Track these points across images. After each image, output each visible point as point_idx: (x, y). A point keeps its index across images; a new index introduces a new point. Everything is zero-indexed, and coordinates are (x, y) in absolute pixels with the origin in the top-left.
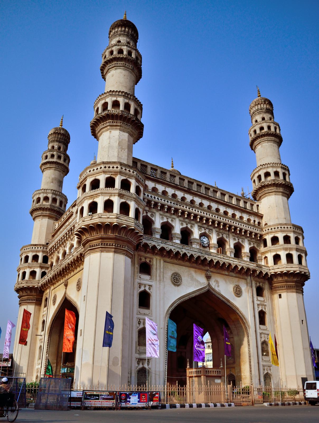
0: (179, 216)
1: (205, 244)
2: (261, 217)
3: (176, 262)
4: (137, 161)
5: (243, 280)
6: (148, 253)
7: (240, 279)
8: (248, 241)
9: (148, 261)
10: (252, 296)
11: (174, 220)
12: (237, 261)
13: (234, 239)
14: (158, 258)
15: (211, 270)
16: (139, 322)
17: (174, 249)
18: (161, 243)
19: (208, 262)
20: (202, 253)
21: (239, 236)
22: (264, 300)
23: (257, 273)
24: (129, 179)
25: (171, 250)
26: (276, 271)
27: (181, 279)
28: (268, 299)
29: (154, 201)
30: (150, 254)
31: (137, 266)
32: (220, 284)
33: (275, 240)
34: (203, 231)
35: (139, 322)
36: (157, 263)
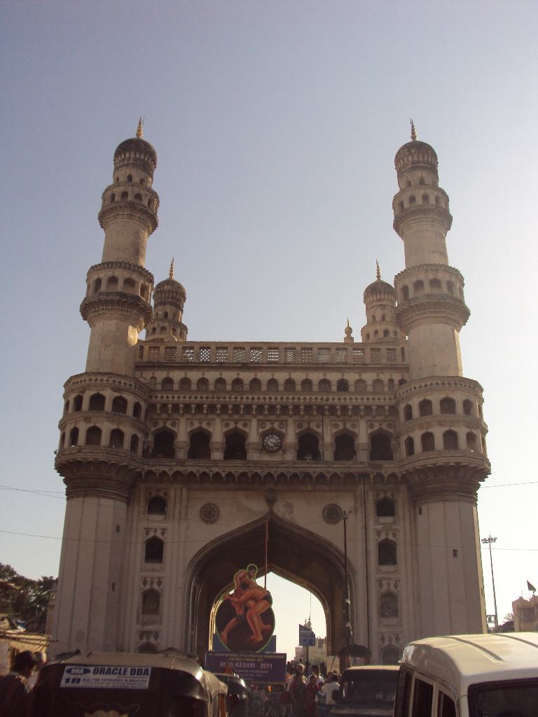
0: (219, 415)
2: (406, 369)
4: (158, 345)
8: (367, 421)
9: (161, 494)
10: (365, 518)
11: (212, 422)
13: (336, 426)
21: (347, 418)
22: (394, 522)
24: (101, 392)
27: (219, 512)
28: (404, 520)
31: (142, 503)
34: (268, 426)
36: (175, 494)
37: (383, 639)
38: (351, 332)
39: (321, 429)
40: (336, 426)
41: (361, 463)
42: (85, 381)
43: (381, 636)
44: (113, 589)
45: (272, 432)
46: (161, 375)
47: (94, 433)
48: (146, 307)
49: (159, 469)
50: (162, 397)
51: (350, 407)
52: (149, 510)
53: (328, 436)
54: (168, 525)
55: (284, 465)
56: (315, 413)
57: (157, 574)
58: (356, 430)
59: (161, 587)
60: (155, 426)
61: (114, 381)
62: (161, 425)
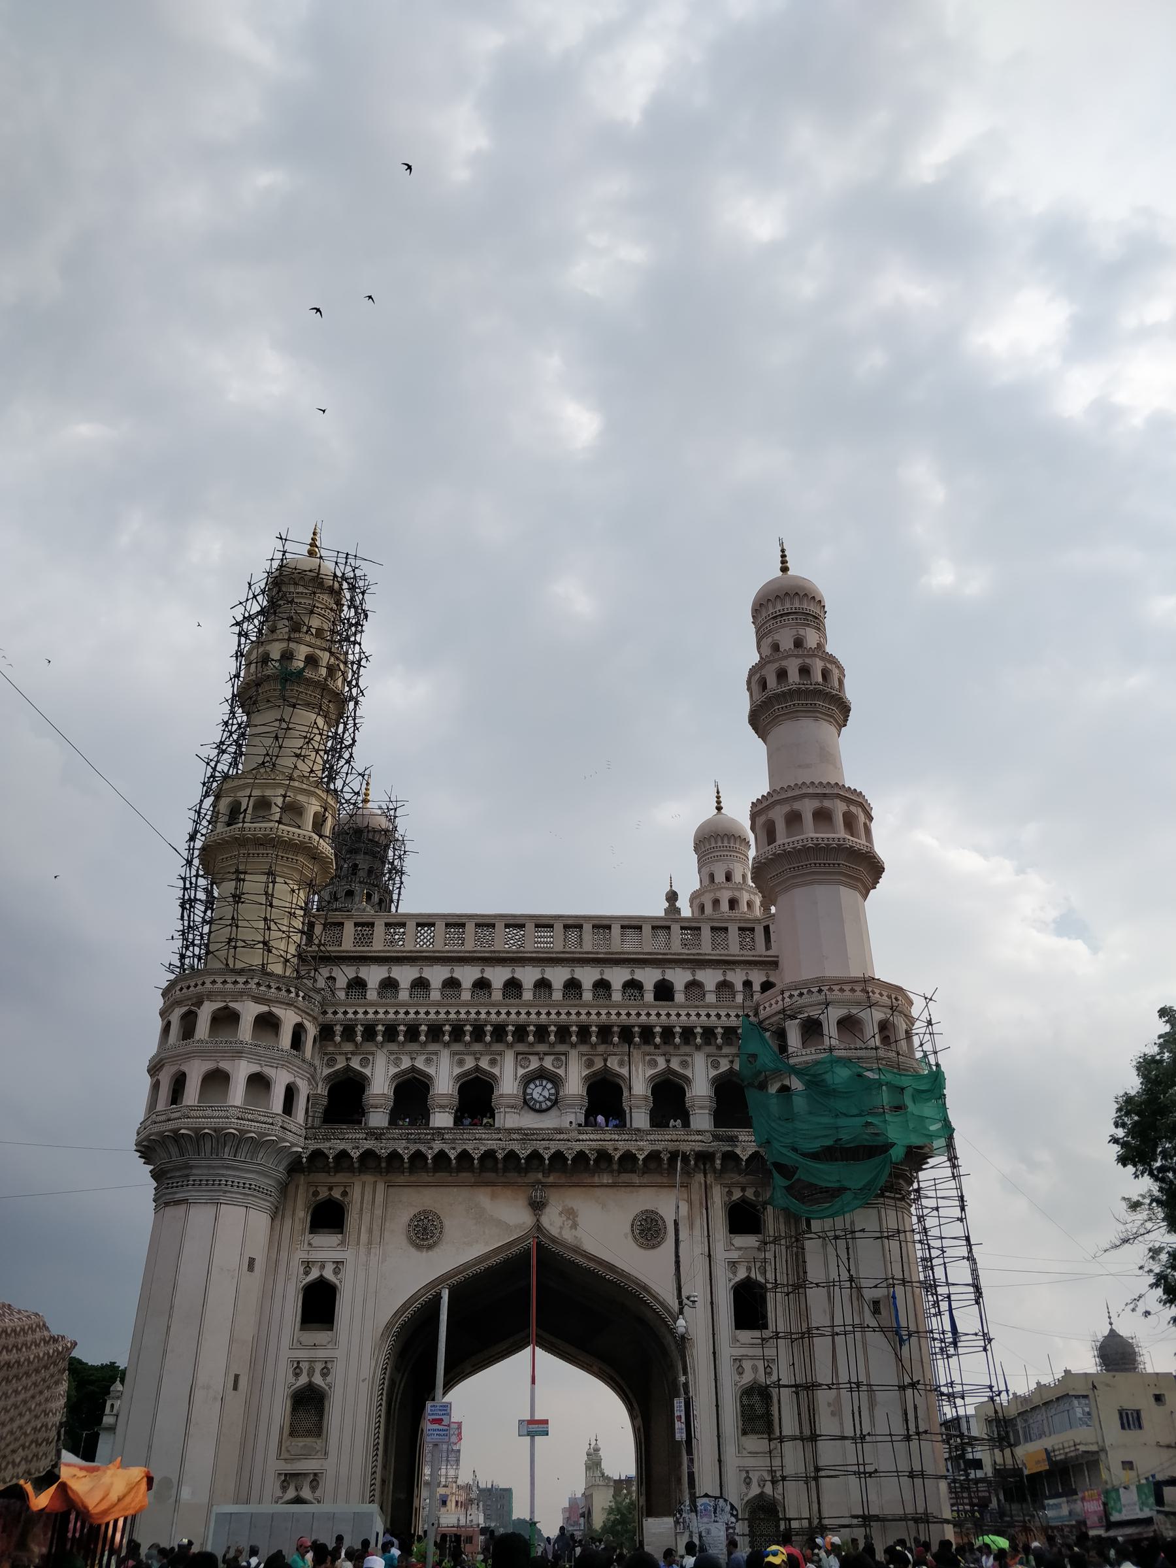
2: (774, 964)
3: (430, 1179)
6: (336, 1172)
10: (708, 1236)
11: (434, 1057)
13: (654, 1063)
14: (369, 1178)
15: (551, 1179)
16: (298, 1371)
21: (670, 1049)
24: (231, 1005)
31: (301, 1214)
32: (578, 1219)
34: (534, 1064)
35: (298, 1371)
36: (364, 1197)
37: (748, 1482)
38: (676, 899)
40: (654, 1063)
41: (699, 1132)
42: (203, 984)
43: (744, 1475)
44: (235, 1388)
45: (541, 1075)
46: (343, 975)
47: (217, 1079)
49: (333, 1147)
50: (345, 1013)
51: (678, 1029)
52: (311, 1227)
53: (639, 1082)
54: (347, 1255)
55: (562, 1136)
56: (616, 1039)
57: (321, 1354)
59: (329, 1379)
60: (329, 1066)
61: (258, 984)
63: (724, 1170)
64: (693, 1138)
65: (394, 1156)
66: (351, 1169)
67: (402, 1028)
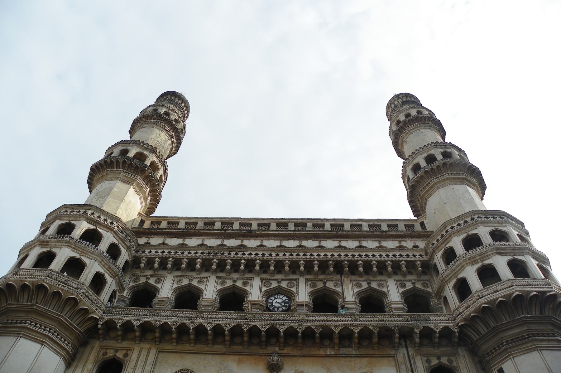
1: (278, 308)
3: (191, 348)
5: (386, 360)
6: (123, 340)
7: (373, 359)
8: (397, 281)
11: (205, 280)
12: (350, 319)
14: (146, 346)
15: (285, 351)
17: (173, 322)
18: (147, 315)
19: (263, 333)
20: (246, 319)
23: (416, 333)
25: (166, 323)
26: (465, 315)
29: (159, 258)
30: (129, 342)
31: (90, 366)
33: (450, 256)
34: (274, 284)
39: (341, 288)
45: (279, 291)
47: (45, 260)
48: (152, 177)
49: (120, 319)
58: (385, 290)
60: (134, 282)
62: (143, 280)
63: (421, 345)
64: (396, 319)
65: (165, 329)
66: (134, 339)
67: (185, 260)
